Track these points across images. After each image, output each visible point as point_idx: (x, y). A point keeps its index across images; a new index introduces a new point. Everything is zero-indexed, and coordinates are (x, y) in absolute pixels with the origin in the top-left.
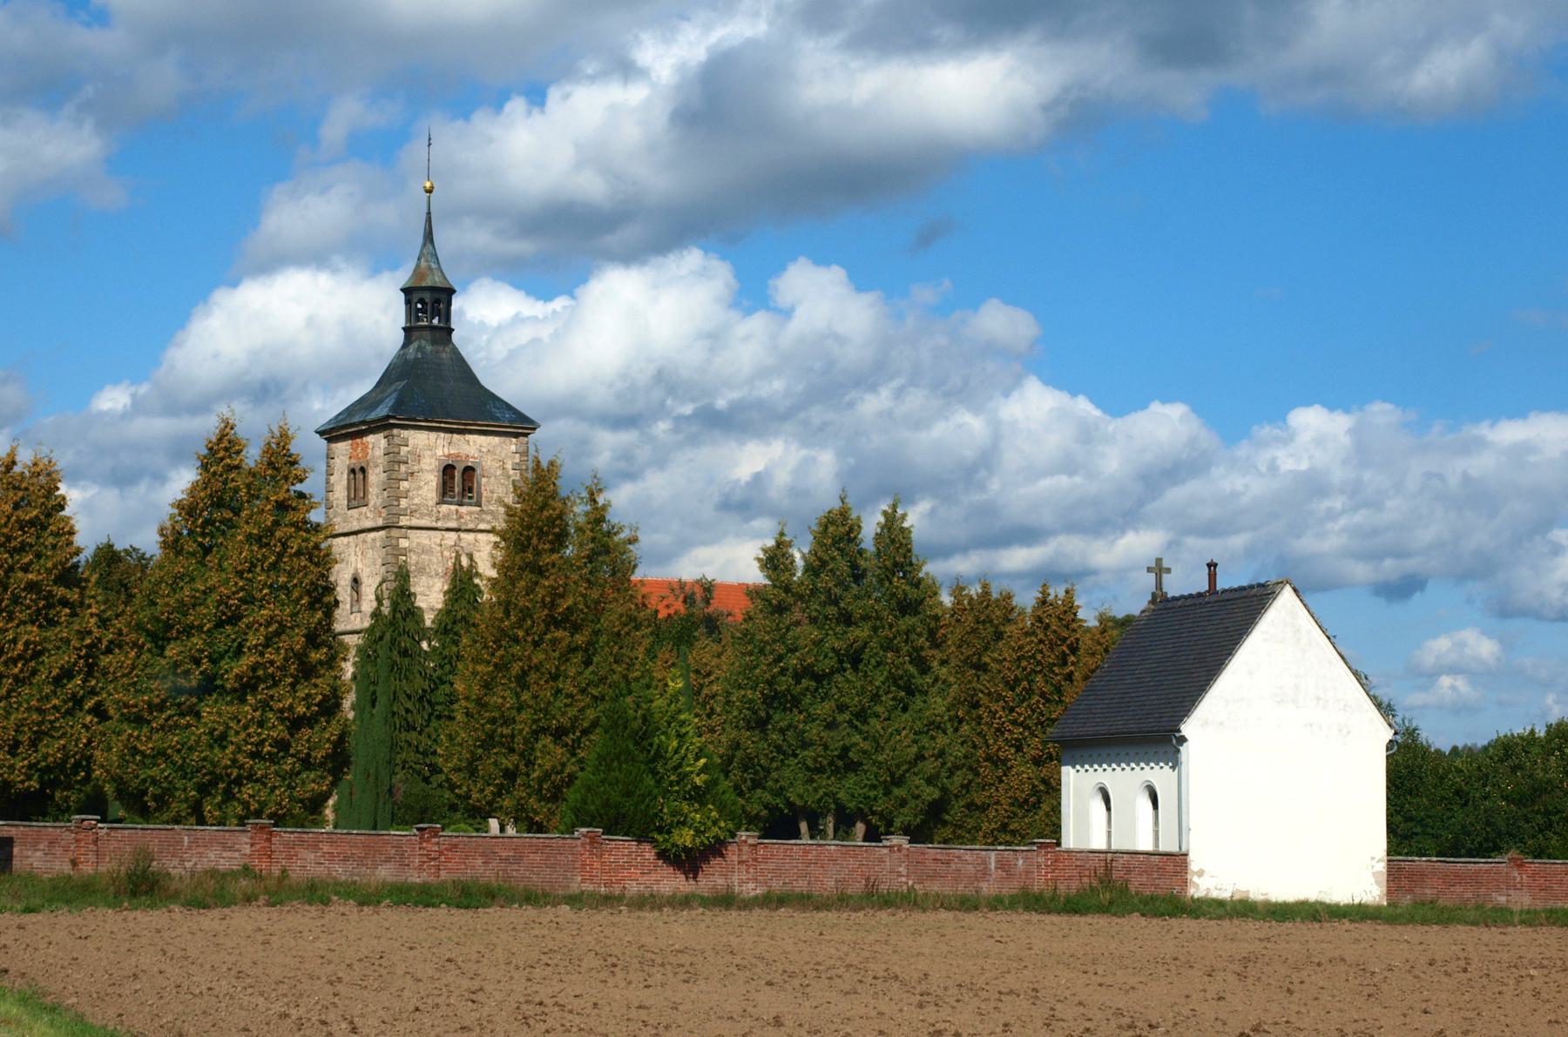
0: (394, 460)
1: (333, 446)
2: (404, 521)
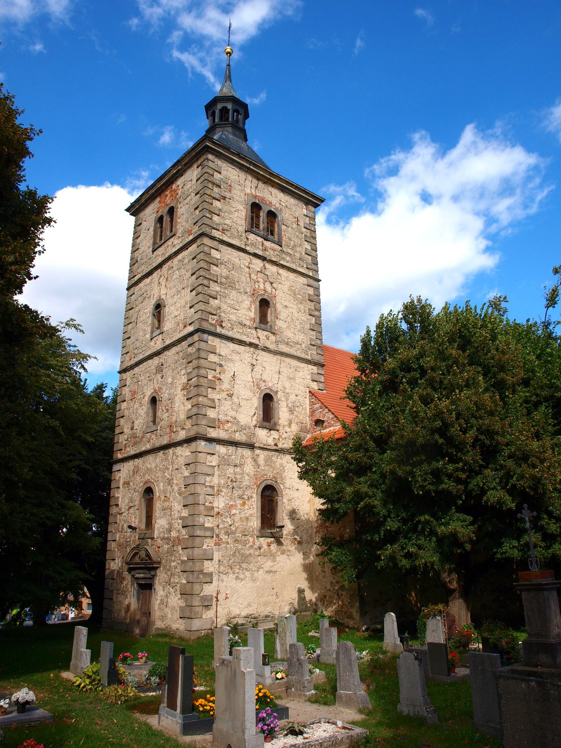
2: (215, 233)
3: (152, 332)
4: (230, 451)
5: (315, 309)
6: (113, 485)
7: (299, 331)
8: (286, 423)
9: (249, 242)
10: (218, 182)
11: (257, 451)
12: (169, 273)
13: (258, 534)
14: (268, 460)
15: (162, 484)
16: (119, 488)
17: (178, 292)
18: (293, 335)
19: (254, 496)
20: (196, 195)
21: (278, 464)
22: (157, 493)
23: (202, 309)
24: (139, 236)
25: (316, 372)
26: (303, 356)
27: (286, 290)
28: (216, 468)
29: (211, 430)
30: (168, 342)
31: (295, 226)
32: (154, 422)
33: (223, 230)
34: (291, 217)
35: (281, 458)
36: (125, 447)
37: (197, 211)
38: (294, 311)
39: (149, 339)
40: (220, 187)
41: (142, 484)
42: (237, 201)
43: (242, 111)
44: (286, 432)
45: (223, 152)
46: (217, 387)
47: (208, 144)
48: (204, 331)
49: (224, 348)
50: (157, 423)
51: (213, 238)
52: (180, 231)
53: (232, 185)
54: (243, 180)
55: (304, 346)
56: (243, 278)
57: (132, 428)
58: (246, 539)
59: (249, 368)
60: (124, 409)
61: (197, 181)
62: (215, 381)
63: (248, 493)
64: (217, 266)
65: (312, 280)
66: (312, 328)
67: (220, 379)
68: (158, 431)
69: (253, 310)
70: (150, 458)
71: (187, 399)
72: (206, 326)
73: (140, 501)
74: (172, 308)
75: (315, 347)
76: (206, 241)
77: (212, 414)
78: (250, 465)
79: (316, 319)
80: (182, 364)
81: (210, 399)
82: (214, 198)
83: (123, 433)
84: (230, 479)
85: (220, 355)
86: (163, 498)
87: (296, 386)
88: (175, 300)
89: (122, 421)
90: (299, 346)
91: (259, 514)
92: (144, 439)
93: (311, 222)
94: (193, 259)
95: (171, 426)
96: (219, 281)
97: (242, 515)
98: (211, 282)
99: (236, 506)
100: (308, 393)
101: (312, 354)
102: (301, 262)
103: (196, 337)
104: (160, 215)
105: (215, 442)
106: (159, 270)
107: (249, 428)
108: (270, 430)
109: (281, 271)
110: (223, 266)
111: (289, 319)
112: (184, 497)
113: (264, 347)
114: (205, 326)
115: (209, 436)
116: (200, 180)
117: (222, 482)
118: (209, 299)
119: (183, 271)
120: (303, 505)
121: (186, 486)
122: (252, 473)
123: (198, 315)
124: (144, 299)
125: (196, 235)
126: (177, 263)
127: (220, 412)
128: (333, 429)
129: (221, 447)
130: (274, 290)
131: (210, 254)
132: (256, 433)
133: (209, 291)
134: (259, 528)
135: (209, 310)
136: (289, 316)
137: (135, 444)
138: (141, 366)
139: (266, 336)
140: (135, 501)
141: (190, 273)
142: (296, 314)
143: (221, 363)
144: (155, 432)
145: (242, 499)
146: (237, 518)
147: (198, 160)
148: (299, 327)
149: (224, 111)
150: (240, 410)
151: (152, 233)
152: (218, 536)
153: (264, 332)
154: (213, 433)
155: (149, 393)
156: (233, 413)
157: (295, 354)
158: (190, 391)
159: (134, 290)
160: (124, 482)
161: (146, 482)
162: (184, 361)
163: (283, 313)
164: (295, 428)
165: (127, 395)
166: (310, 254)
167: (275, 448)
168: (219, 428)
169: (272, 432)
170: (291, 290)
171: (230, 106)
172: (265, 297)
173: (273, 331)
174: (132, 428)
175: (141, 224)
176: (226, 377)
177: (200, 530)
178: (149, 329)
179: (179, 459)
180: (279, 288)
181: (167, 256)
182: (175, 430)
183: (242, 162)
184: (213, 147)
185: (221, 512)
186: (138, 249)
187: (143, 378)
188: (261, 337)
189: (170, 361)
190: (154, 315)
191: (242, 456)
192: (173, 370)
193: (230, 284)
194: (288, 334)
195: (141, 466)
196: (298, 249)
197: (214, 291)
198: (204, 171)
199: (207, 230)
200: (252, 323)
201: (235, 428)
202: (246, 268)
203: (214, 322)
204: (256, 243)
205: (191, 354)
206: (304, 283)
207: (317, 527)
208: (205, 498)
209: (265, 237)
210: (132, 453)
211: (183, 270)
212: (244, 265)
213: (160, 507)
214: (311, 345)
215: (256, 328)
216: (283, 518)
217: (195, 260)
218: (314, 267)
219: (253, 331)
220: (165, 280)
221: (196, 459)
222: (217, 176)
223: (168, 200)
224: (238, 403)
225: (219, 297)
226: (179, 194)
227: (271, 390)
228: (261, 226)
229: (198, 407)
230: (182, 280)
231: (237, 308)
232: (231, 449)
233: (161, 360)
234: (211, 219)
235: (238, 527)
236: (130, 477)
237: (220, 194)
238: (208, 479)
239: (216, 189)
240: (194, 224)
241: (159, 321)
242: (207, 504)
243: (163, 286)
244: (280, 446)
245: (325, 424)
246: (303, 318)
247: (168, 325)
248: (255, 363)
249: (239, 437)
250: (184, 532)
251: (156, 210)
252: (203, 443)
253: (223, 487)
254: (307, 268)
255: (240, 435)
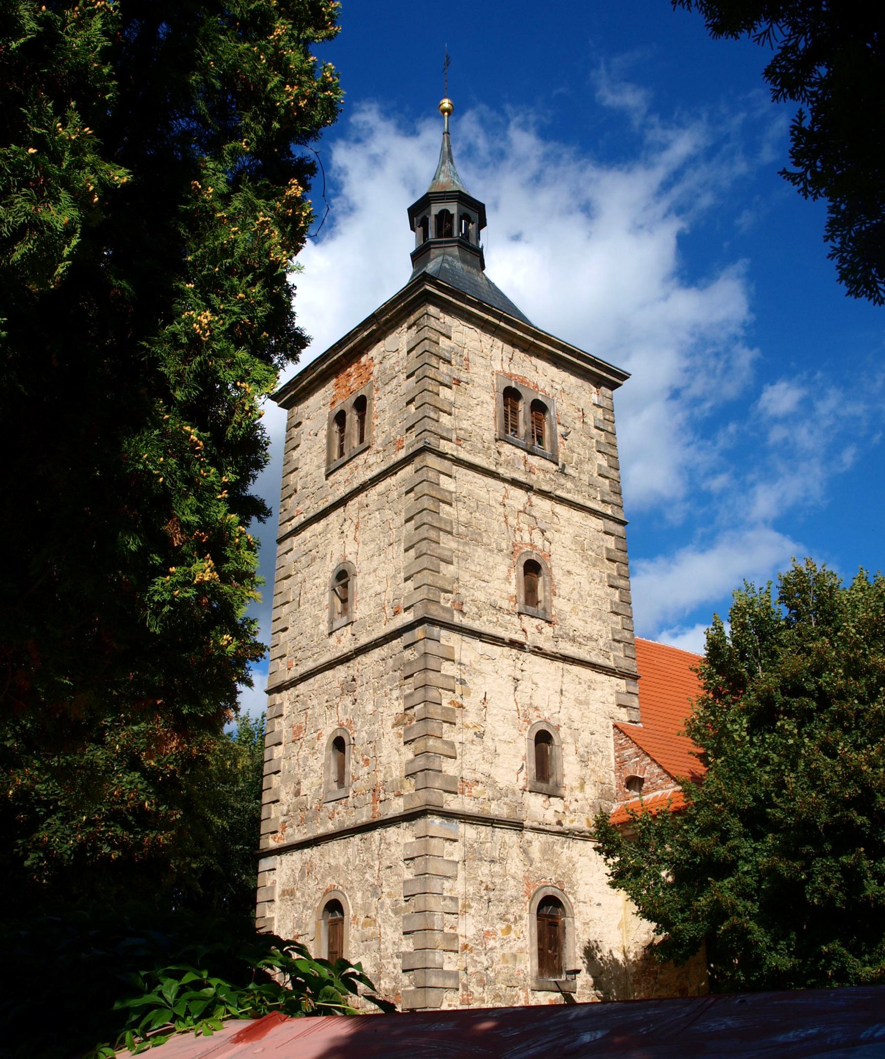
0: (426, 354)
1: (300, 409)
2: (446, 447)
3: (331, 621)
4: (483, 835)
5: (619, 575)
6: (260, 897)
7: (593, 616)
8: (576, 784)
9: (503, 458)
10: (447, 354)
11: (529, 835)
12: (362, 514)
13: (534, 985)
14: (547, 850)
15: (359, 895)
16: (272, 901)
17: (381, 550)
18: (582, 623)
19: (526, 915)
20: (408, 377)
21: (564, 857)
22: (350, 911)
23: (429, 582)
24: (298, 446)
25: (624, 689)
26: (601, 661)
27: (568, 543)
28: (460, 866)
29: (449, 797)
30: (364, 640)
31: (578, 425)
32: (341, 782)
33: (458, 439)
34: (571, 409)
35: (569, 847)
36: (284, 829)
37: (412, 408)
38: (584, 581)
39: (326, 633)
40: (449, 362)
41: (319, 895)
42: (480, 385)
43: (475, 216)
44: (576, 800)
45: (454, 301)
46: (457, 721)
47: (428, 288)
48: (433, 622)
49: (468, 650)
50: (346, 784)
51: (442, 455)
52: (379, 441)
53: (470, 357)
54: (489, 347)
55: (601, 644)
56: (495, 525)
57: (297, 793)
58: (514, 993)
59: (510, 685)
60: (280, 758)
61: (409, 352)
62: (453, 711)
63: (515, 909)
64: (451, 505)
65: (611, 523)
66: (614, 609)
67: (461, 706)
68: (350, 799)
69: (514, 582)
70: (335, 846)
71: (405, 743)
72: (436, 613)
73: (317, 924)
74: (371, 579)
75: (622, 645)
76: (431, 460)
77: (450, 768)
78: (517, 860)
79: (621, 592)
80: (393, 679)
81: (446, 742)
82: (442, 384)
83: (277, 801)
84: (484, 885)
85: (460, 664)
86: (362, 919)
87: (590, 714)
88: (375, 564)
89: (275, 780)
90: (594, 643)
91: (535, 948)
92: (322, 814)
93: (607, 417)
94: (407, 493)
95: (374, 791)
96: (454, 531)
97: (506, 950)
98: (441, 533)
99: (495, 933)
100: (611, 728)
101: (616, 658)
102: (592, 491)
103: (419, 632)
104: (338, 409)
105: (457, 818)
106: (341, 509)
107: (514, 793)
108: (550, 796)
109: (560, 509)
110: (460, 504)
111: (575, 596)
112: (404, 918)
113: (535, 647)
114: (435, 612)
115: (446, 807)
116: (414, 352)
117: (471, 890)
118: (439, 565)
119: (388, 514)
120: (610, 932)
121: (408, 897)
122: (520, 875)
123: (422, 594)
124: (314, 559)
125: (411, 451)
126: (376, 498)
127: (464, 766)
128: (663, 793)
129: (468, 826)
130: (547, 543)
131: (438, 484)
132: (526, 803)
133: (438, 551)
134: (534, 975)
135: (440, 583)
136: (574, 589)
137: (303, 821)
138: (311, 680)
139: (537, 627)
140: (307, 925)
141: (403, 517)
142: (586, 586)
143: (463, 677)
144: (343, 801)
145: (506, 920)
146: (497, 955)
147: (409, 315)
148: (592, 608)
149: (444, 216)
150: (496, 761)
151: (325, 441)
152: (465, 987)
153: (533, 619)
154: (453, 803)
155: (328, 730)
156: (485, 767)
157: (588, 658)
158: (410, 728)
159: (292, 543)
160: (283, 891)
161: (327, 891)
162: (398, 673)
163: (565, 586)
164: (591, 792)
165: (284, 732)
166: (606, 474)
167: (557, 828)
168: (463, 793)
169: (552, 799)
170: (576, 543)
171: (453, 208)
172: (534, 557)
173: (549, 618)
174: (297, 793)
175: (300, 424)
176: (472, 703)
177: (437, 976)
178: (325, 615)
179: (393, 849)
180: (556, 539)
181: (355, 486)
182: (382, 797)
183: (486, 317)
184: (437, 292)
185: (471, 945)
186: (296, 469)
187: (315, 702)
188: (527, 629)
189: (369, 674)
190: (334, 590)
191: (504, 844)
192: (375, 690)
193: (473, 536)
194: (575, 622)
195: (316, 861)
196: (586, 467)
197: (448, 549)
198: (423, 335)
199: (432, 440)
200: (512, 604)
201: (490, 794)
202: (498, 506)
203: (449, 605)
204: (514, 461)
205: (410, 663)
206: (599, 528)
207: (636, 972)
208: (443, 919)
209: (528, 449)
210: (299, 837)
211: (387, 512)
212: (496, 500)
213: (357, 935)
214: (614, 640)
215: (520, 614)
216: (574, 957)
217: (412, 495)
218: (614, 498)
219: (515, 619)
220: (353, 528)
221: (426, 849)
222: (444, 342)
223: (353, 383)
224: (493, 748)
225: (455, 560)
226: (375, 373)
227: (548, 724)
228: (522, 429)
229: (428, 757)
230: (387, 529)
231: (487, 578)
232: (485, 831)
233: (351, 672)
234: (437, 421)
235: (499, 972)
236: (295, 881)
237: (450, 376)
238: (447, 884)
239: (444, 368)
240: (407, 430)
241: (344, 601)
242: (446, 930)
243: (351, 536)
244: (567, 824)
245: (645, 785)
246: (599, 593)
247: (361, 610)
248: (519, 677)
249: (496, 810)
250: (405, 979)
251: (330, 399)
252: (437, 820)
253: (472, 899)
254: (603, 501)
255: (499, 805)
